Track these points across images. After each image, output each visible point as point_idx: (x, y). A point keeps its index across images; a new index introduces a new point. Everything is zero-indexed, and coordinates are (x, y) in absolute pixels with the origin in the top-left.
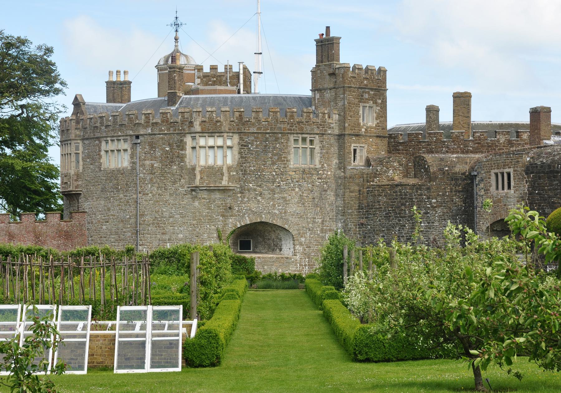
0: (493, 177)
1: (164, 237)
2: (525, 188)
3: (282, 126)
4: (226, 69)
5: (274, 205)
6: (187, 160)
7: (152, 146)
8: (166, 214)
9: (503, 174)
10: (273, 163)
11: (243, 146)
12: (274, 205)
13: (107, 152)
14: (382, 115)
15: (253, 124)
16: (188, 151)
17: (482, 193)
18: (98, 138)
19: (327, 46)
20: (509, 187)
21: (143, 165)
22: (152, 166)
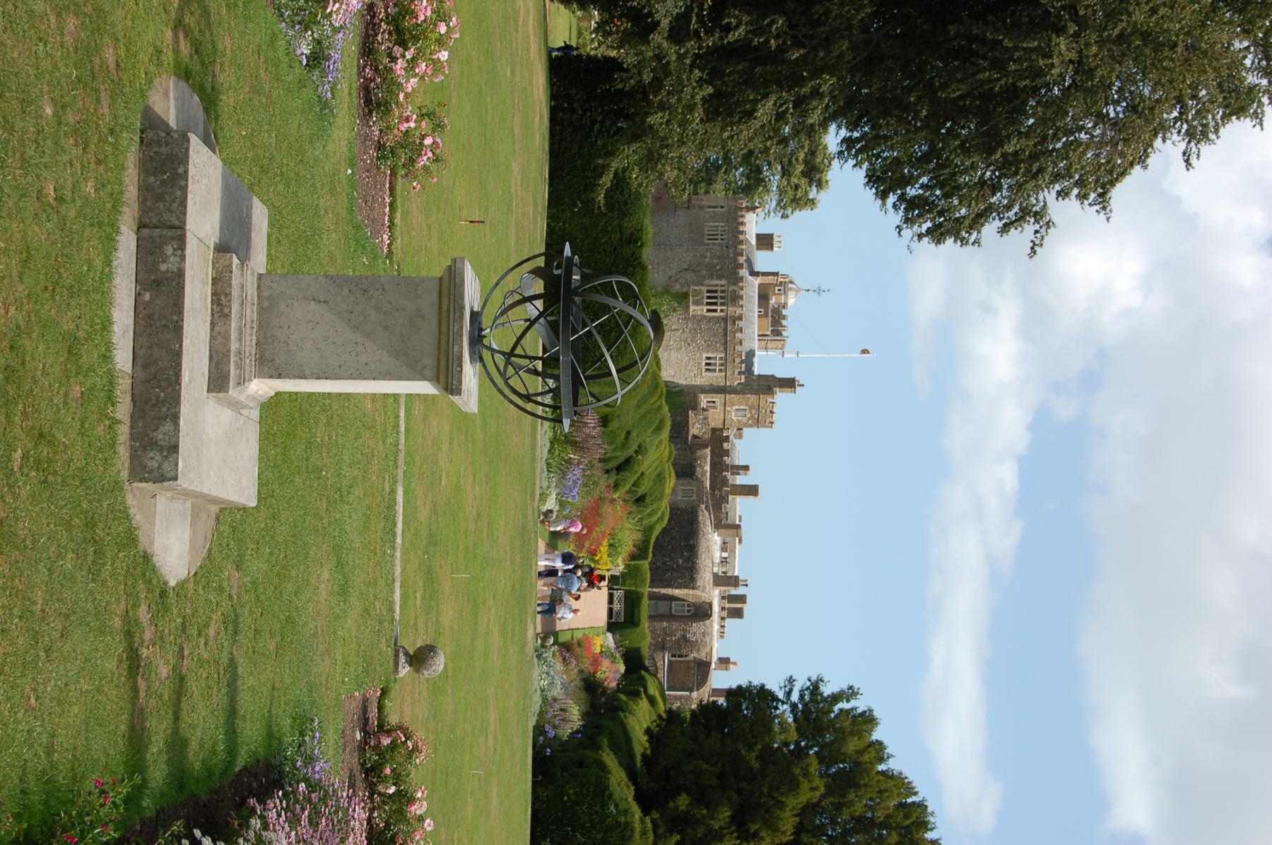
2: (683, 506)
7: (719, 257)
19: (790, 384)
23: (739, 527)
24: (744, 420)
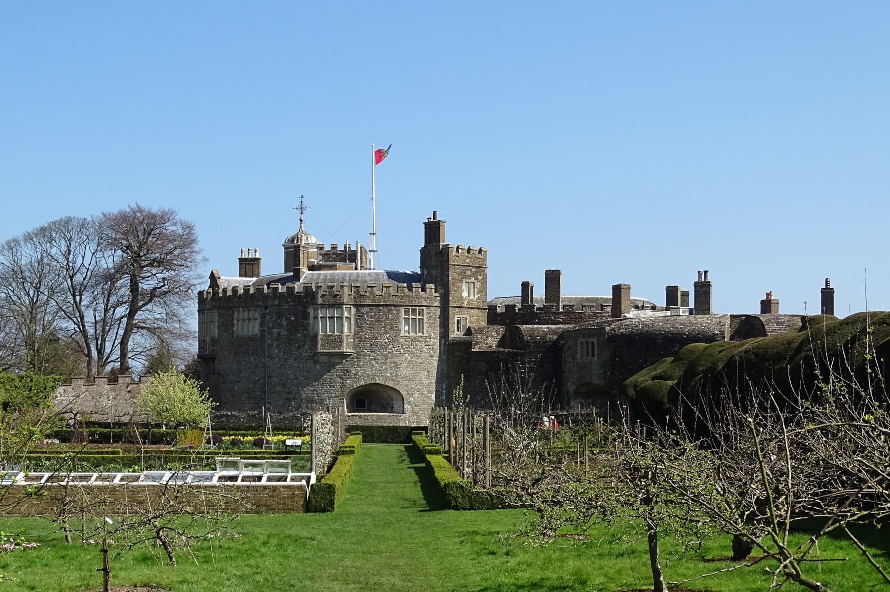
0: (579, 346)
1: (289, 396)
3: (395, 299)
4: (345, 247)
5: (386, 369)
6: (310, 329)
8: (291, 376)
9: (588, 343)
10: (386, 333)
11: (359, 316)
12: (386, 369)
13: (238, 320)
14: (483, 290)
15: (369, 297)
16: (311, 320)
17: (570, 359)
18: (231, 309)
19: (433, 229)
20: (593, 355)
21: (270, 333)
22: (279, 332)
23: (617, 289)
24: (478, 284)
